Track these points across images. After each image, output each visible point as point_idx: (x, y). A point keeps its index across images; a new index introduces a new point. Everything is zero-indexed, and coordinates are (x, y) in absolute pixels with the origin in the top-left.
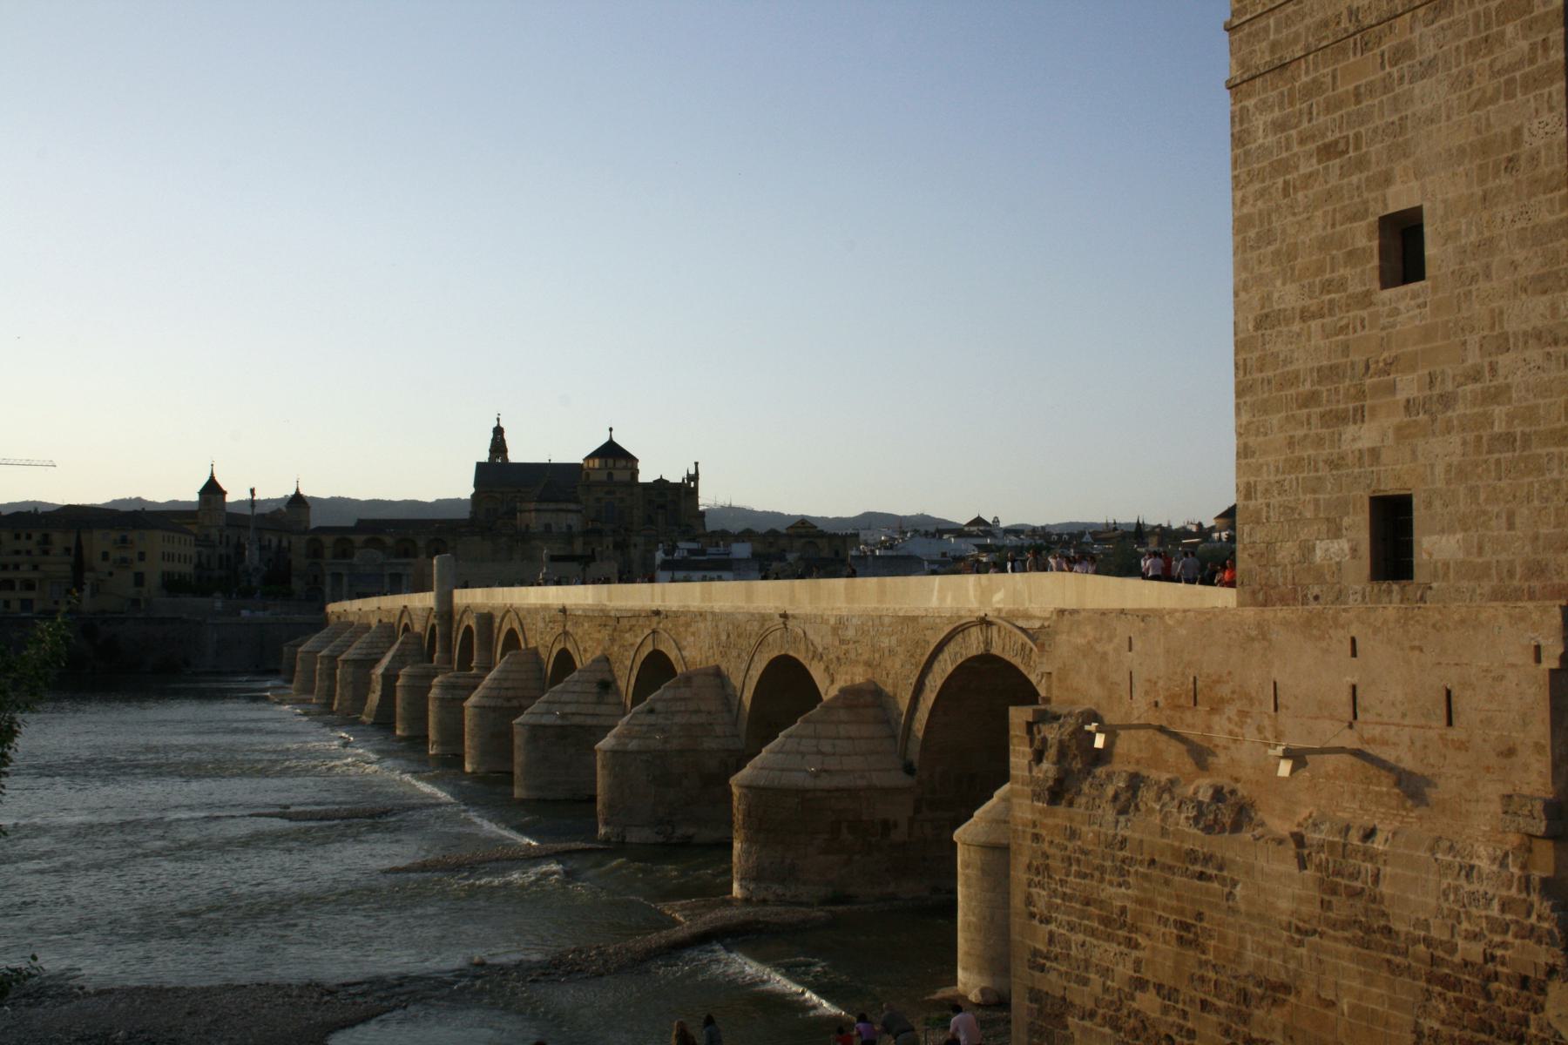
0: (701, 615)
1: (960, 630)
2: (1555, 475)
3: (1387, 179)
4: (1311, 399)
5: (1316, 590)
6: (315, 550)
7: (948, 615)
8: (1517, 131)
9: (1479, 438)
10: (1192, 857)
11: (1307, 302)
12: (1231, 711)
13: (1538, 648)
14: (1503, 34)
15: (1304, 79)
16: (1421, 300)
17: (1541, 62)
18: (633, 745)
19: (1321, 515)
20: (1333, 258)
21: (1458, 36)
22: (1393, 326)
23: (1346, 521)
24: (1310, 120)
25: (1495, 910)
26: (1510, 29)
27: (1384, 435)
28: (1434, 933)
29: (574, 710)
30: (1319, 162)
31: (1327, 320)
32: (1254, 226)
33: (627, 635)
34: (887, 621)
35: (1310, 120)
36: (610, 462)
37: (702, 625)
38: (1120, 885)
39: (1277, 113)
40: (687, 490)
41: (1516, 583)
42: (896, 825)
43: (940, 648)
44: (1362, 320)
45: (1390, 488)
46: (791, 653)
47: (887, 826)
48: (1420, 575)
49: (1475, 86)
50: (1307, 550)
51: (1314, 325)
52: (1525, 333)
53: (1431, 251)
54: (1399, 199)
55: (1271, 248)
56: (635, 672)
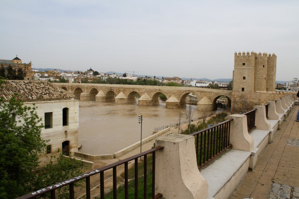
1: (187, 91)
4: (239, 83)
36: (18, 60)
40: (30, 65)
54: (244, 76)
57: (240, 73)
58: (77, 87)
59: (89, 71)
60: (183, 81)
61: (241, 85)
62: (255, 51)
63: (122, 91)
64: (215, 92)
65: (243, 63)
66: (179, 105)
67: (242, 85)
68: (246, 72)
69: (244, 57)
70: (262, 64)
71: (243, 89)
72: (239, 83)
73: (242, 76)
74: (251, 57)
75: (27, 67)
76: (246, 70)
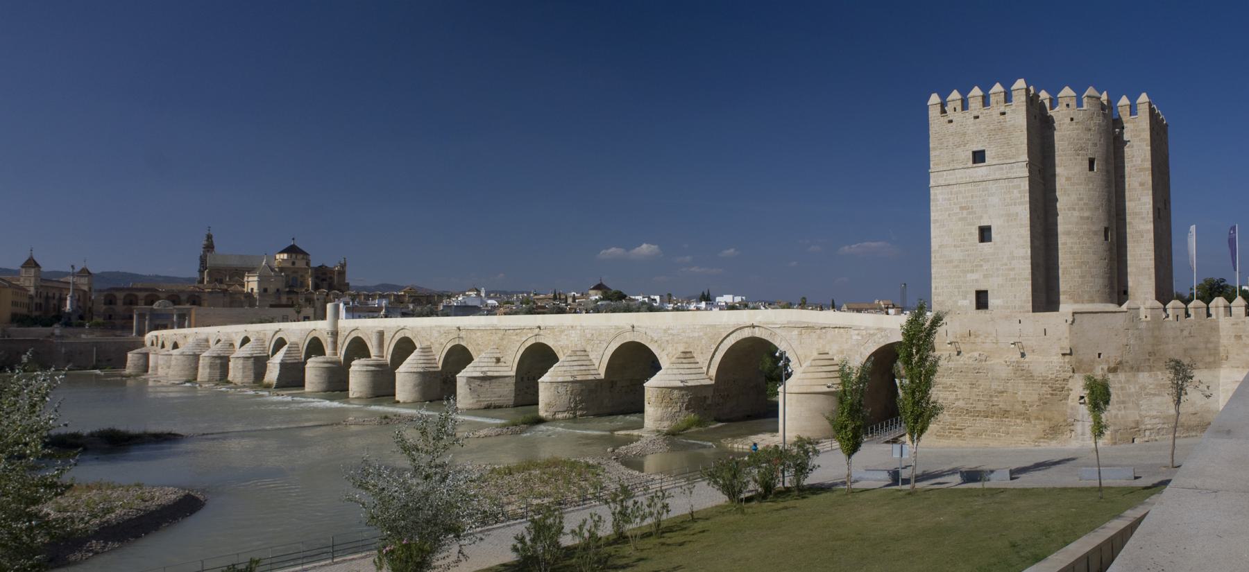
0: (572, 327)
3: (981, 217)
4: (957, 266)
5: (958, 312)
6: (110, 301)
7: (733, 324)
8: (1017, 213)
9: (1007, 279)
10: (974, 369)
12: (982, 337)
15: (955, 190)
17: (1023, 200)
18: (560, 379)
23: (968, 296)
25: (1058, 368)
28: (1043, 374)
34: (697, 327)
37: (573, 332)
39: (946, 196)
42: (708, 398)
43: (728, 336)
45: (982, 288)
46: (638, 340)
47: (705, 398)
48: (989, 307)
53: (993, 235)
54: (985, 223)
55: (944, 229)
56: (521, 352)
57: (962, 208)
58: (354, 335)
61: (971, 277)
64: (866, 329)
65: (975, 153)
66: (709, 402)
69: (977, 117)
72: (957, 266)
73: (974, 225)
75: (302, 276)
76: (992, 187)
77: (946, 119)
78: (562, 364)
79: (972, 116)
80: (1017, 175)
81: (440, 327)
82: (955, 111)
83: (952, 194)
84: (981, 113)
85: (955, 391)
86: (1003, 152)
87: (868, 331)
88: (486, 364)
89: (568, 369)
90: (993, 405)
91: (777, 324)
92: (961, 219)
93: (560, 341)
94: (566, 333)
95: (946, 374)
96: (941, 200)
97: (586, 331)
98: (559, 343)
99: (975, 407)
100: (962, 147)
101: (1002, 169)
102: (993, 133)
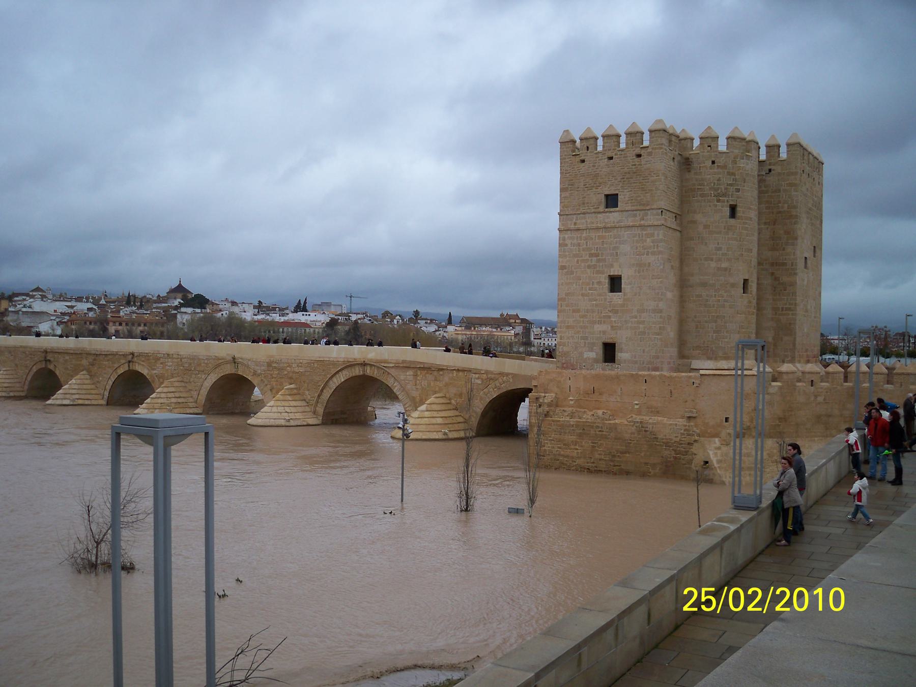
0: (168, 355)
2: (656, 342)
3: (612, 266)
8: (649, 263)
9: (635, 332)
11: (584, 292)
13: (693, 382)
14: (646, 240)
16: (620, 297)
19: (587, 346)
20: (593, 282)
21: (634, 237)
22: (611, 302)
24: (587, 245)
26: (648, 240)
27: (608, 328)
28: (667, 437)
29: (78, 398)
30: (589, 257)
31: (590, 297)
32: (566, 269)
33: (104, 363)
34: (305, 362)
35: (587, 245)
38: (571, 436)
41: (644, 365)
44: (602, 301)
49: (638, 250)
50: (581, 354)
51: (585, 298)
52: (650, 310)
54: (614, 272)
55: (572, 276)
57: (591, 255)
59: (172, 295)
60: (527, 331)
61: (598, 328)
62: (677, 126)
63: (88, 371)
64: (487, 372)
65: (607, 196)
67: (603, 327)
68: (625, 248)
69: (611, 158)
70: (719, 196)
71: (609, 352)
73: (603, 273)
74: (650, 154)
77: (578, 159)
78: (158, 396)
79: (606, 157)
80: (650, 223)
81: (25, 347)
82: (588, 150)
83: (581, 240)
84: (616, 154)
85: (577, 449)
86: (637, 197)
87: (489, 376)
88: (74, 391)
89: (166, 401)
90: (615, 466)
91: (388, 363)
92: (589, 267)
93: (154, 369)
94: (161, 362)
95: (567, 431)
96: (569, 245)
97: (183, 360)
98: (155, 372)
99: (596, 467)
100: (594, 190)
101: (635, 216)
102: (628, 176)
